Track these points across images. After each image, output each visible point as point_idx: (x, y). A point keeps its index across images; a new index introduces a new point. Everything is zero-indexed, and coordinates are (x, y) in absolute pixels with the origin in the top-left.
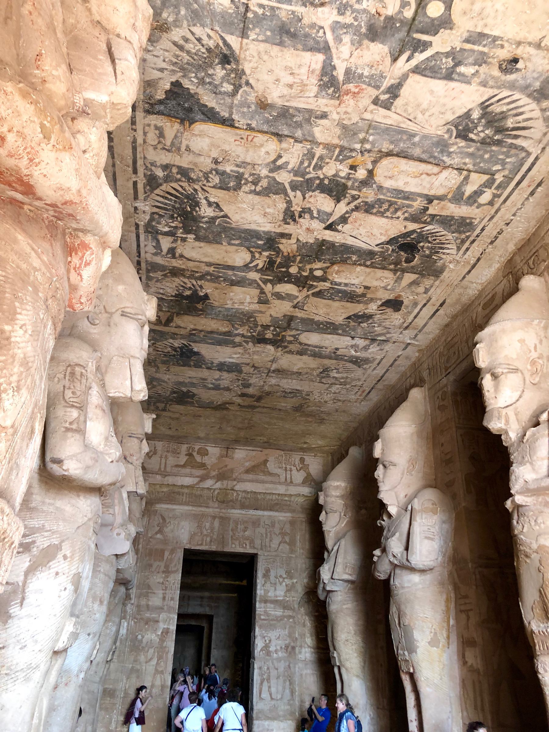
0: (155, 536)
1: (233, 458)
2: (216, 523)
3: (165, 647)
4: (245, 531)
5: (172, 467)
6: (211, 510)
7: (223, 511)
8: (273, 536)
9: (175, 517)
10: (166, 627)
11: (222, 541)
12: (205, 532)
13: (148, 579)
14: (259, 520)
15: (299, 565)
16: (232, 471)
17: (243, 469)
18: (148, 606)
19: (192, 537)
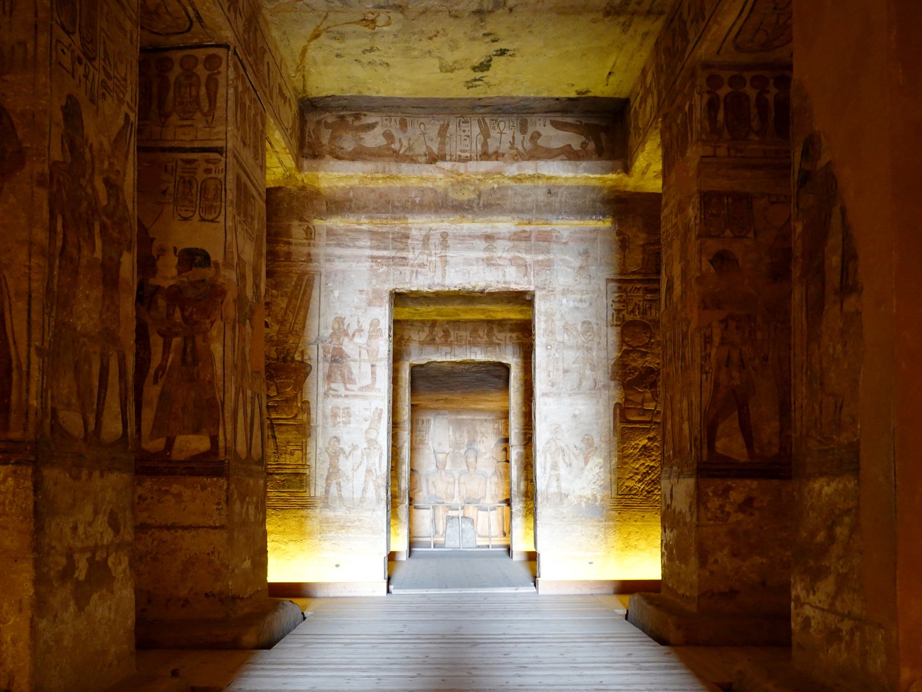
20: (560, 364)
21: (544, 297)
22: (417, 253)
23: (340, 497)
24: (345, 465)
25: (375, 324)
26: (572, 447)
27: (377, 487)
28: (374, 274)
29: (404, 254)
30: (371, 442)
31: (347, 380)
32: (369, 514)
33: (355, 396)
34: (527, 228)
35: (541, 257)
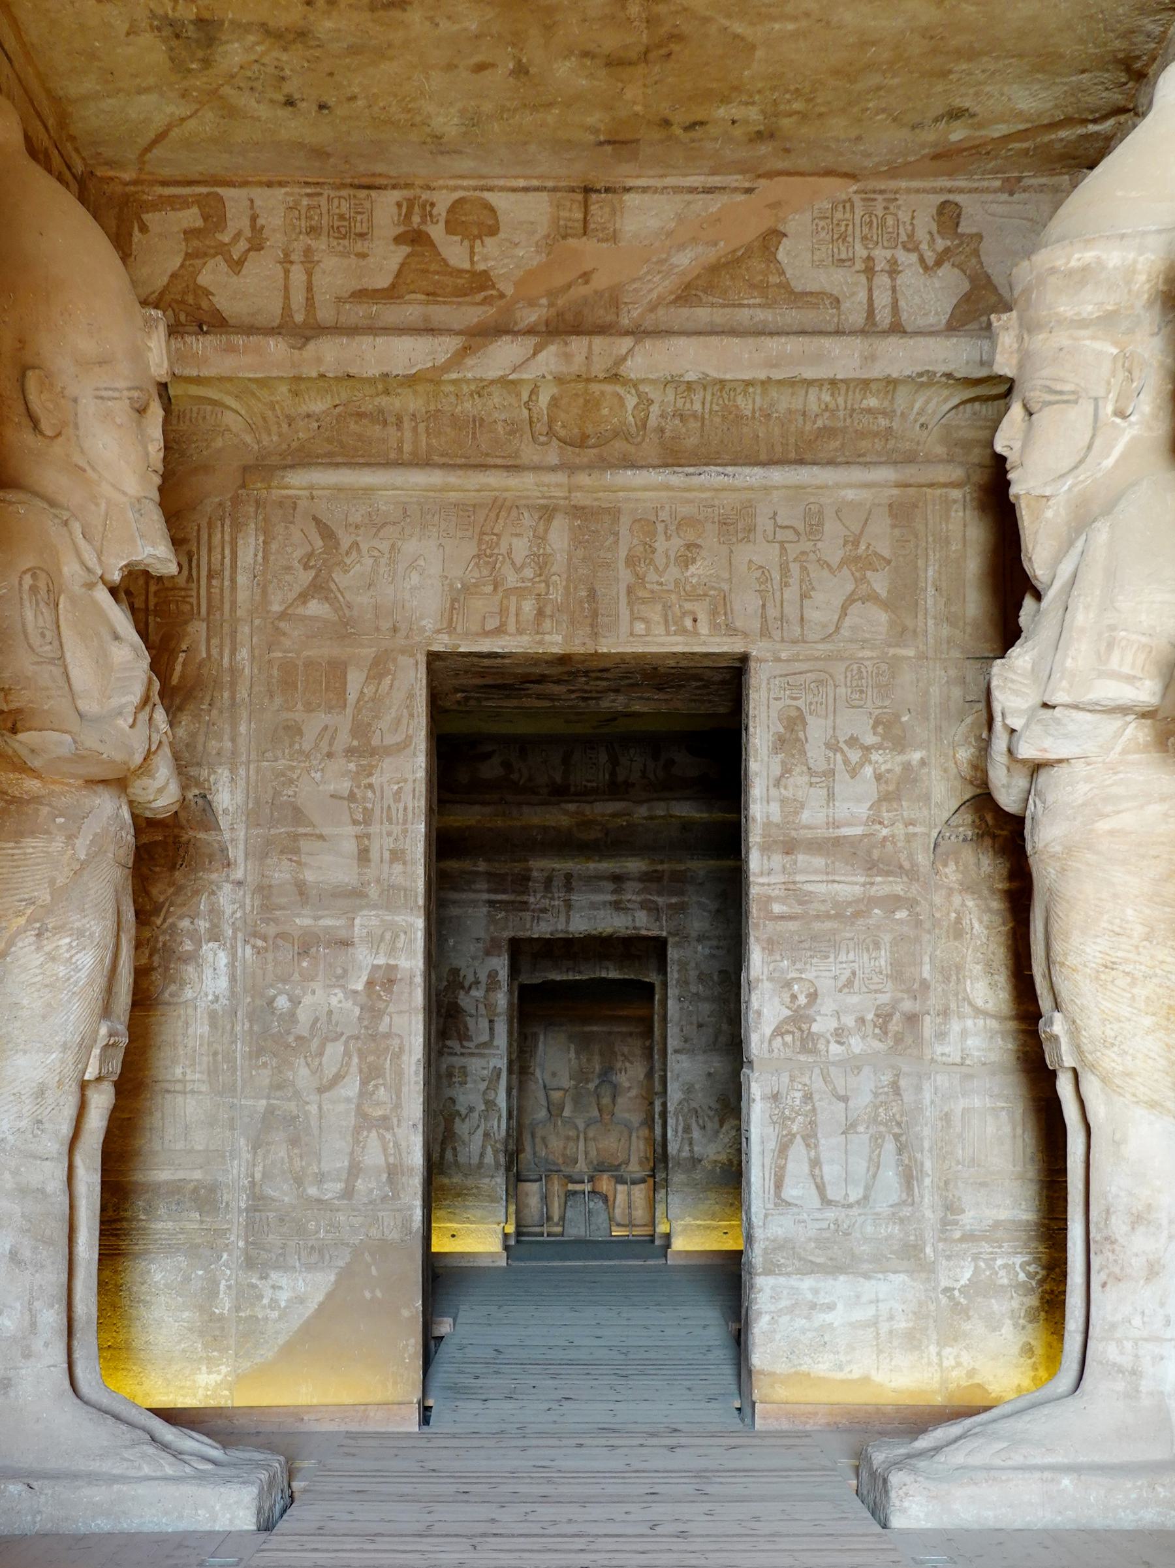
0: (300, 610)
1: (614, 237)
2: (559, 537)
3: (387, 1036)
4: (685, 562)
5: (339, 299)
6: (529, 479)
7: (583, 479)
8: (815, 572)
9: (377, 524)
10: (381, 961)
11: (591, 610)
12: (512, 580)
13: (291, 781)
14: (747, 509)
15: (934, 690)
16: (614, 299)
17: (662, 286)
18: (301, 889)
19: (457, 601)
20: (694, 1018)
21: (677, 945)
22: (538, 896)
23: (456, 1161)
24: (462, 1128)
25: (493, 975)
26: (705, 1108)
27: (496, 1152)
28: (491, 919)
29: (525, 898)
30: (490, 1104)
31: (464, 1036)
32: (487, 1180)
33: (472, 1054)
34: (659, 867)
35: (674, 900)
